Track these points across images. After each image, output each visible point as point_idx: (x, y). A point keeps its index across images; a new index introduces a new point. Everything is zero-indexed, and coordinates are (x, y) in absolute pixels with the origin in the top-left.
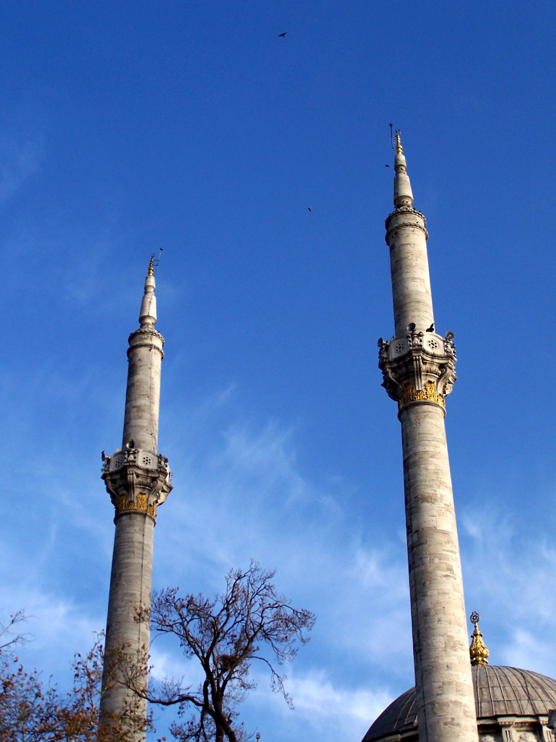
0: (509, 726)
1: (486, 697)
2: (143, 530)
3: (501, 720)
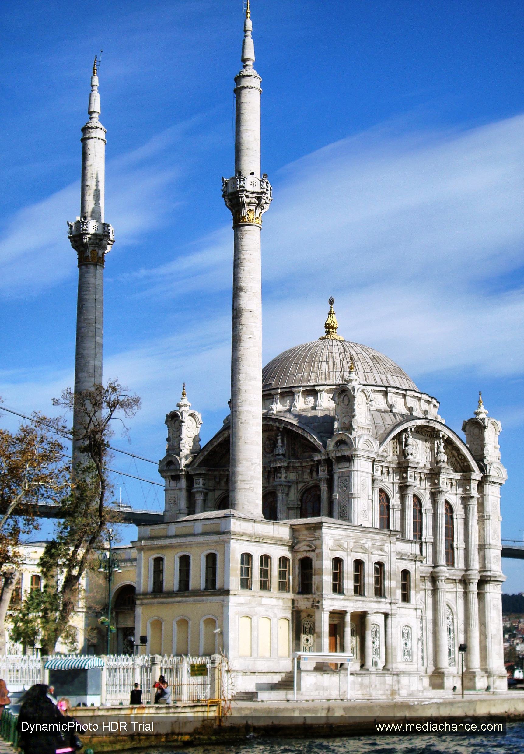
0: (322, 391)
1: (315, 369)
2: (95, 275)
3: (317, 388)
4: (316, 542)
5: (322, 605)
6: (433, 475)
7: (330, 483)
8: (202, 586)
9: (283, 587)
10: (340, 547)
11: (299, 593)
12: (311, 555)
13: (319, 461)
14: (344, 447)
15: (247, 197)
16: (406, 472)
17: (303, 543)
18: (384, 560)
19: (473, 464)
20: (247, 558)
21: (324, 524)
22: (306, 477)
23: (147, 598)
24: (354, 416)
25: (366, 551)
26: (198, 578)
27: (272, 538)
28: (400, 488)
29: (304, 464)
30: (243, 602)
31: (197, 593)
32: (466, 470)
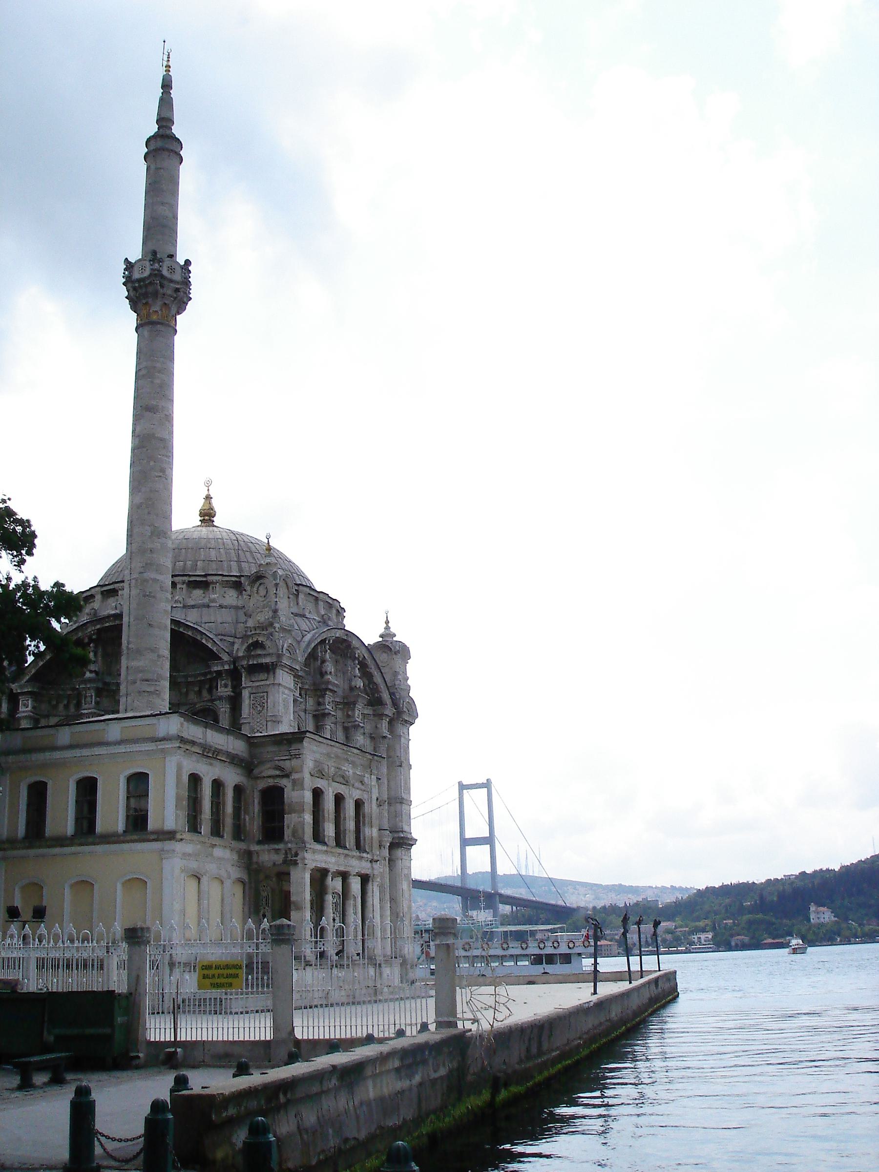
3: (210, 578)
4: (294, 762)
5: (304, 858)
6: (348, 704)
7: (235, 702)
8: (121, 827)
9: (239, 833)
10: (320, 773)
11: (259, 843)
12: (284, 782)
13: (219, 673)
14: (259, 652)
15: (162, 286)
16: (323, 696)
17: (268, 765)
18: (365, 797)
19: (386, 696)
20: (195, 780)
21: (308, 735)
22: (192, 697)
23: (16, 849)
24: (275, 611)
25: (346, 783)
26: (112, 812)
27: (228, 754)
28: (315, 716)
29: (189, 679)
30: (191, 852)
31: (109, 838)
32: (375, 702)
